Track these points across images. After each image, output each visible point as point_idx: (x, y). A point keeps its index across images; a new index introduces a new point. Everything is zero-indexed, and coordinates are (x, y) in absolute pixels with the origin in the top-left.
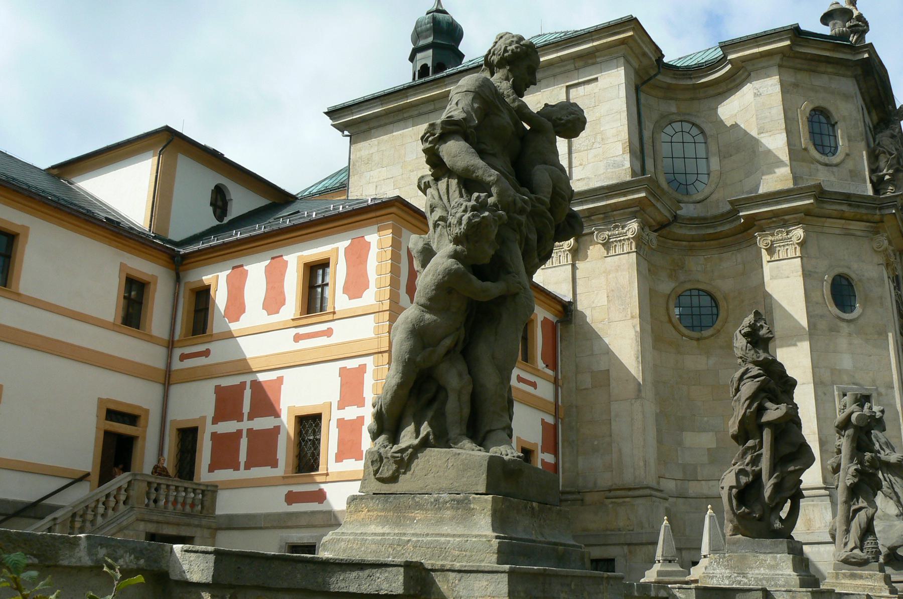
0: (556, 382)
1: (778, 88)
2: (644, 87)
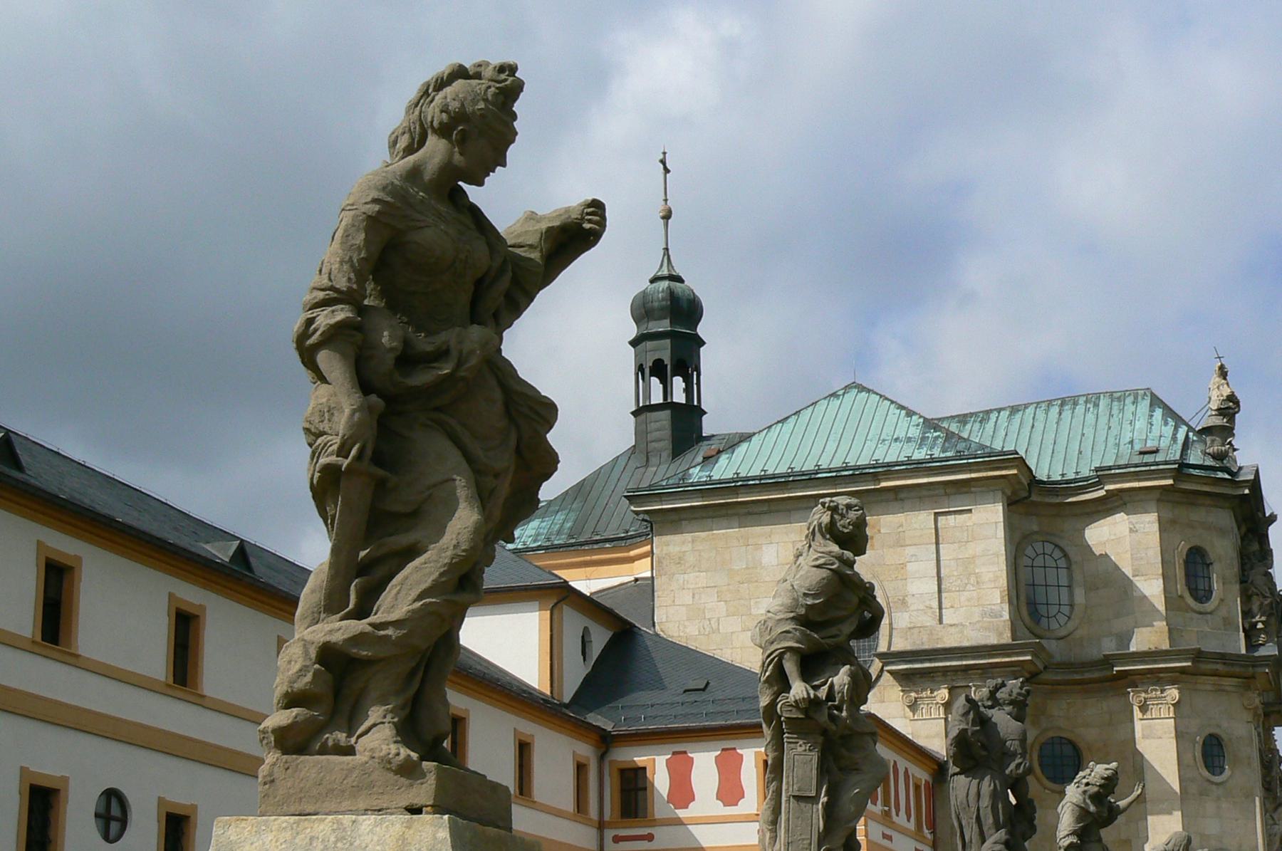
1: (1156, 526)
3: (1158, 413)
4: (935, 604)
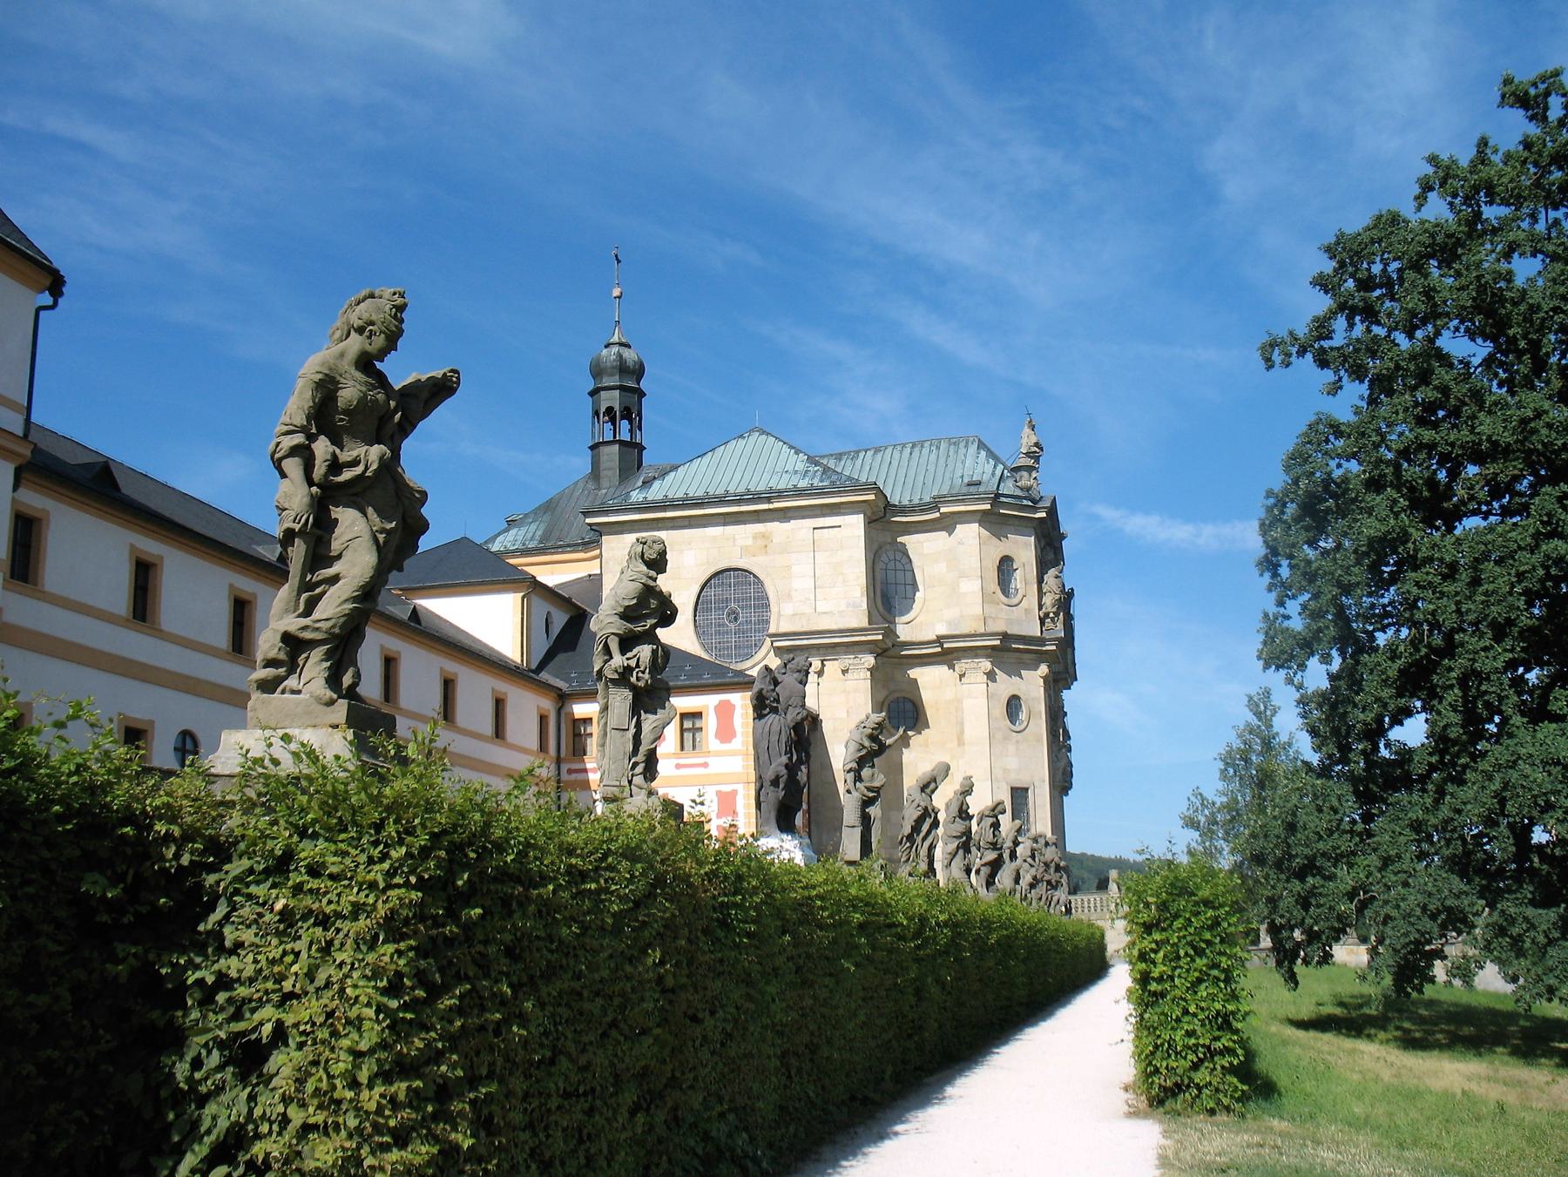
3: (983, 453)
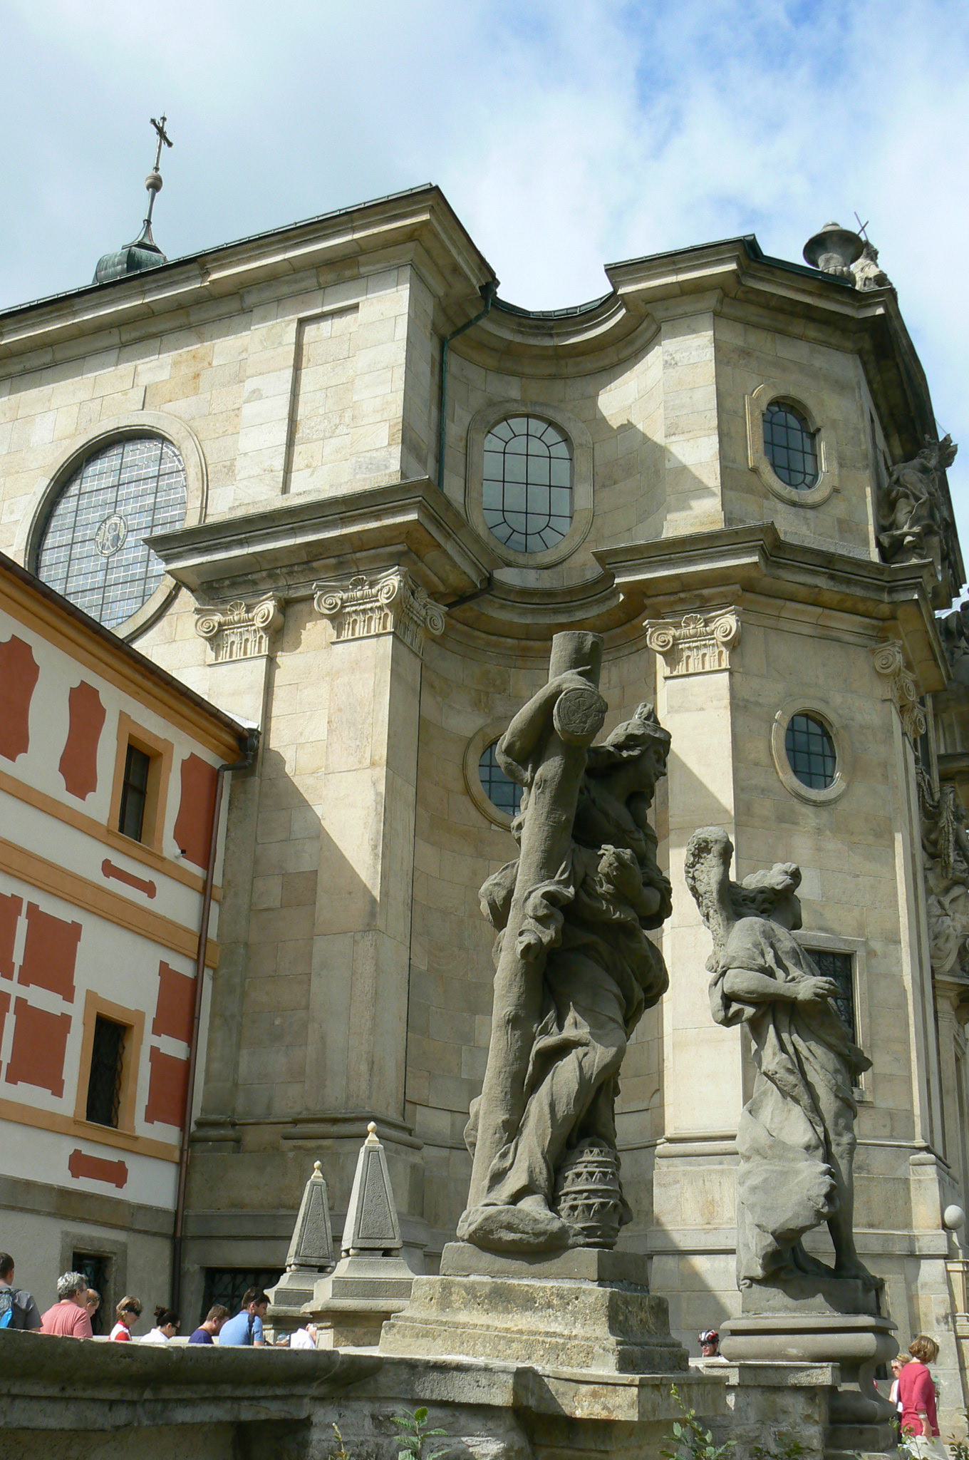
0: (206, 891)
1: (710, 353)
2: (456, 342)
4: (279, 463)
